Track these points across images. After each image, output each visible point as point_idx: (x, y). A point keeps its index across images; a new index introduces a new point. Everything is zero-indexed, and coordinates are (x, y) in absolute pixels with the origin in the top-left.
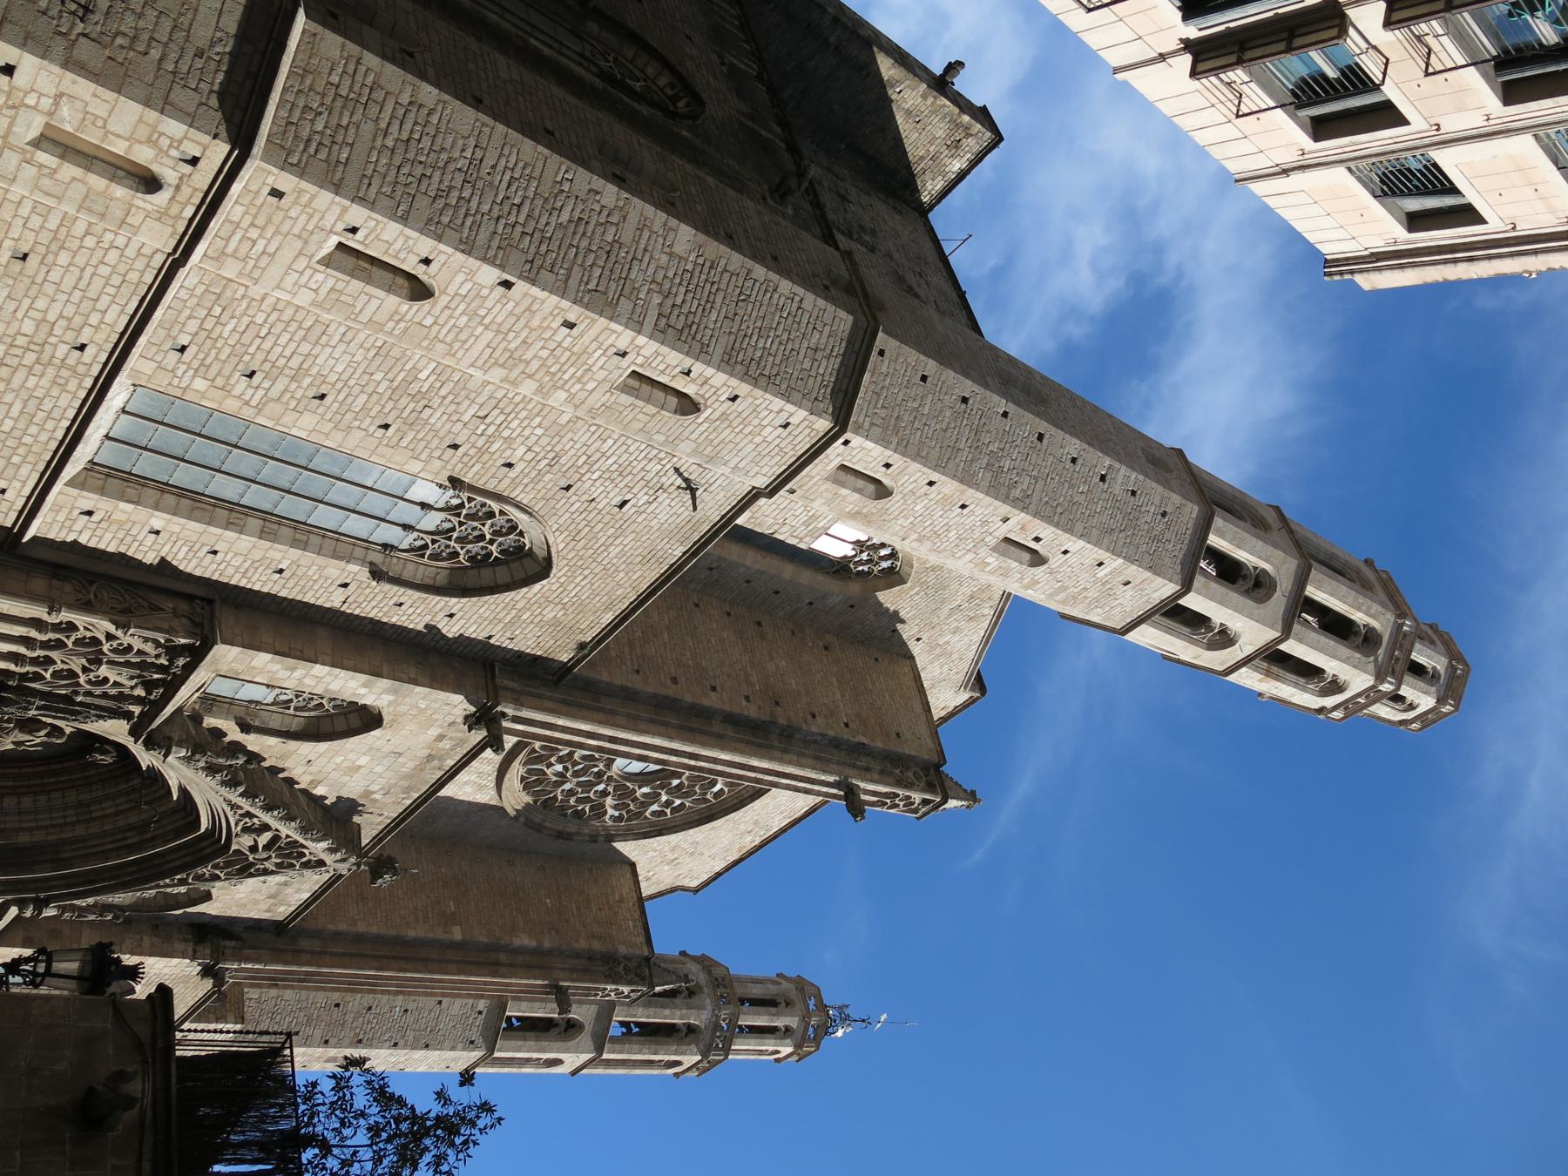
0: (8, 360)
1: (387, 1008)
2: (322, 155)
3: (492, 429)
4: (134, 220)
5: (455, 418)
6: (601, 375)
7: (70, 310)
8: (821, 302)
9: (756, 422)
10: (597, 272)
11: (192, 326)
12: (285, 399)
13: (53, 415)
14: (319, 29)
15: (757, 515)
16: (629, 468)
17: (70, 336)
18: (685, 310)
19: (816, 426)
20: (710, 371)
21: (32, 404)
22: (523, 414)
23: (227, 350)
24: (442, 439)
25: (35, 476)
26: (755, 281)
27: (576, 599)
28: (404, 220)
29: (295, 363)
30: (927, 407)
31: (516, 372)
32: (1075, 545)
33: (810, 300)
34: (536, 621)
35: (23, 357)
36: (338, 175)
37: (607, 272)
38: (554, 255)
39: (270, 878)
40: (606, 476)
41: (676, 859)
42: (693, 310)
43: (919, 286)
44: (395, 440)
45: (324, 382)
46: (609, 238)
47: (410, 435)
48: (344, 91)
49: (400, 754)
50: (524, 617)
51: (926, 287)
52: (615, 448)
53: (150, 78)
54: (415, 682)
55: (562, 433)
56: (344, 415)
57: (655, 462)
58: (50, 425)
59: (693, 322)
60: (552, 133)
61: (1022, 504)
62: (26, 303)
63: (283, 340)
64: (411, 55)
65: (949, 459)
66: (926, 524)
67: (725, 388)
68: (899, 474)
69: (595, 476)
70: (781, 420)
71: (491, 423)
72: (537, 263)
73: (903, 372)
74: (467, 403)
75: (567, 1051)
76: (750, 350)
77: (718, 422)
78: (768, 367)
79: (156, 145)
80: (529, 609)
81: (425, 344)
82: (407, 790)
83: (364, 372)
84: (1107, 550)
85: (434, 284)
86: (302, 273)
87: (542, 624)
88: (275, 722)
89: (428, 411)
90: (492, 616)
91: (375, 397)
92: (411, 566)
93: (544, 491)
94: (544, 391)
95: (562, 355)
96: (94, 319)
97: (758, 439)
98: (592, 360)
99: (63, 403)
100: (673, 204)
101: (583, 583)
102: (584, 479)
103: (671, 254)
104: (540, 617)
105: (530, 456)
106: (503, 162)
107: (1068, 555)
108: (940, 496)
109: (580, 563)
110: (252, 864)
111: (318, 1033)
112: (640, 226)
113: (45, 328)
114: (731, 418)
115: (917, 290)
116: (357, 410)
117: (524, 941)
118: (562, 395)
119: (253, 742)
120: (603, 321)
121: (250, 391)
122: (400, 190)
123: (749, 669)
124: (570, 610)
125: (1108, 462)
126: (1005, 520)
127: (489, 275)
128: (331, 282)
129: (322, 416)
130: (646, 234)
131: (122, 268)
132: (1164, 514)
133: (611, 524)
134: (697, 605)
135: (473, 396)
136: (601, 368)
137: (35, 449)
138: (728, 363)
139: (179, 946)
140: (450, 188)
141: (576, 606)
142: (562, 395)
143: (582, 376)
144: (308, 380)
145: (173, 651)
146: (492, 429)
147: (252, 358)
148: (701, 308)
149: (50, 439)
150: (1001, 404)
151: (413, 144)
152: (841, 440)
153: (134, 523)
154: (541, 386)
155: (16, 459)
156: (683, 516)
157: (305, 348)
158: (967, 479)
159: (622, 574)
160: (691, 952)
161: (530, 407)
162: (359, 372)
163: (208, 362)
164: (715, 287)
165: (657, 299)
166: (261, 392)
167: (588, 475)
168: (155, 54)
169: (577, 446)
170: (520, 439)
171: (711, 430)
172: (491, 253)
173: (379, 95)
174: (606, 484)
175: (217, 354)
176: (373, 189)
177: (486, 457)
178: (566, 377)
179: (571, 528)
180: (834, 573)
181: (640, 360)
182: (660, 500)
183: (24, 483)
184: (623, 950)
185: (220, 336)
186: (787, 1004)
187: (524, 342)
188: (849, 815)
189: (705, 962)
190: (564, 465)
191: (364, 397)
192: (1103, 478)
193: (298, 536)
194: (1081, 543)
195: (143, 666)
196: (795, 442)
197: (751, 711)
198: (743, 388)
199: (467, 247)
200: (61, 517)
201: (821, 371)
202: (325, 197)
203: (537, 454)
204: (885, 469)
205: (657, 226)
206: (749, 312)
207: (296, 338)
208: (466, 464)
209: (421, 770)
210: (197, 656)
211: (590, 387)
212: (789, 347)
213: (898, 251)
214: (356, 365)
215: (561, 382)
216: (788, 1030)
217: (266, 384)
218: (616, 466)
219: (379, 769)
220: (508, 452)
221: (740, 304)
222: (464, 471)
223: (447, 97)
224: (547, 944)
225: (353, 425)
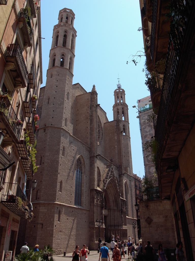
11: (69, 202)
20: (61, 147)
28: (56, 186)
29: (69, 191)
32: (66, 90)
54: (94, 166)
60: (41, 172)
61: (63, 99)
64: (39, 189)
75: (127, 126)
84: (65, 84)
100: (44, 156)
103: (50, 155)
111: (128, 158)
117: (116, 138)
120: (59, 161)
127: (59, 175)
130: (48, 159)
132: (59, 75)
134: (77, 130)
138: (59, 145)
139: (121, 179)
158: (63, 108)
165: (55, 156)
166: (73, 193)
184: (115, 124)
186: (118, 94)
189: (114, 107)
192: (57, 86)
194: (66, 88)
195: (98, 195)
197: (89, 122)
198: (61, 142)
199: (57, 179)
202: (57, 194)
224: (116, 135)
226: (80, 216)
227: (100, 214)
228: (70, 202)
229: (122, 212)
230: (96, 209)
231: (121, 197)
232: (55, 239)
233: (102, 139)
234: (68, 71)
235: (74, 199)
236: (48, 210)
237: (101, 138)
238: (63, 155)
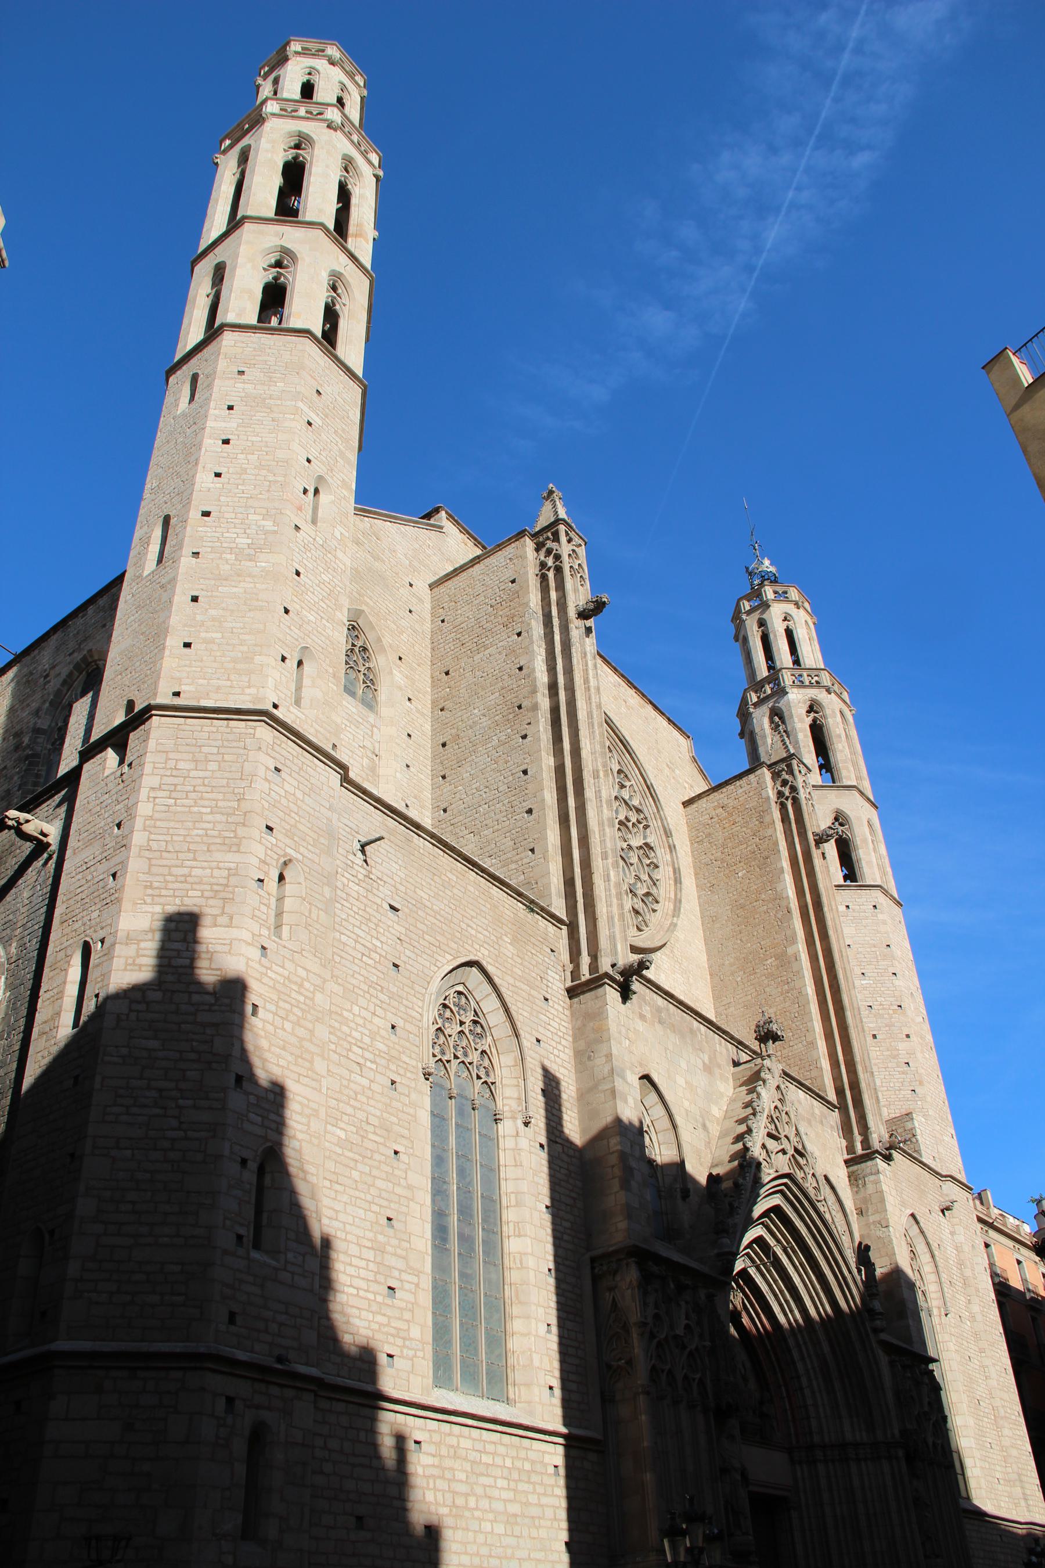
0: (449, 1502)
1: (865, 992)
3: (367, 1055)
5: (370, 1093)
6: (288, 964)
8: (148, 768)
9: (284, 801)
12: (404, 1253)
13: (481, 1449)
15: (364, 775)
16: (361, 912)
19: (270, 740)
22: (345, 1029)
23: (379, 1318)
24: (391, 1099)
26: (149, 840)
27: (489, 929)
29: (370, 1255)
30: (215, 635)
31: (313, 1048)
34: (519, 960)
35: (442, 1490)
38: (194, 1044)
39: (802, 1130)
40: (374, 933)
41: (668, 765)
42: (199, 894)
43: (59, 674)
44: (405, 1142)
45: (376, 1223)
49: (666, 1049)
50: (520, 973)
51: (57, 668)
52: (348, 933)
55: (351, 987)
56: (399, 1196)
57: (347, 890)
58: (490, 1448)
59: (212, 890)
60: (76, 1078)
65: (258, 600)
66: (324, 606)
67: (264, 841)
68: (287, 646)
69: (379, 944)
70: (272, 776)
71: (362, 1057)
73: (188, 669)
74: (352, 1085)
76: (219, 827)
77: (296, 838)
78: (229, 804)
80: (512, 971)
81: (316, 1141)
83: (356, 1189)
85: (261, 1149)
86: (293, 1273)
87: (520, 955)
89: (373, 1120)
90: (528, 1003)
91: (375, 1172)
93: (406, 989)
94: (320, 1015)
95: (284, 1009)
97: (299, 794)
98: (279, 978)
99: (465, 1443)
100: (102, 941)
101: (474, 926)
102: (384, 954)
104: (515, 957)
105: (379, 1011)
107: (311, 458)
108: (295, 599)
109: (457, 934)
110: (796, 1150)
111: (903, 1046)
112: (137, 968)
114: (288, 827)
115: (63, 676)
116: (390, 1185)
118: (319, 997)
121: (407, 1286)
123: (494, 743)
124: (500, 930)
125: (207, 442)
129: (406, 1214)
133: (415, 915)
135: (345, 1083)
136: (283, 967)
137: (514, 1454)
139: (871, 1188)
141: (495, 927)
142: (319, 997)
143: (296, 983)
144: (380, 1238)
146: (367, 1055)
147: (378, 1294)
148: (195, 886)
149: (502, 1444)
152: (275, 711)
153: (548, 1349)
154: (318, 1020)
155: (527, 1466)
156: (388, 848)
159: (455, 891)
160: (739, 729)
161: (337, 1025)
162: (357, 1193)
163: (393, 1331)
164: (169, 878)
166: (405, 1276)
167: (378, 950)
169: (357, 969)
170: (368, 1025)
171: (305, 844)
174: (382, 931)
175: (385, 1325)
177: (394, 1053)
178: (302, 999)
179: (429, 952)
180: (373, 684)
181: (265, 932)
182: (379, 875)
183: (544, 1452)
185: (368, 1328)
187: (284, 1048)
188: (604, 610)
190: (378, 977)
191: (379, 1183)
192: (226, 442)
193: (513, 1203)
196: (291, 758)
201: (215, 750)
203: (376, 1005)
204: (287, 661)
206: (181, 838)
207: (348, 1260)
208: (406, 1069)
209: (673, 1026)
211: (303, 973)
212: (201, 788)
213: (28, 705)
214: (353, 1199)
215: (308, 1001)
217: (396, 1273)
218: (364, 927)
219: (684, 1065)
220: (383, 1033)
221: (177, 849)
222: (412, 1069)
225: (405, 1184)
226: (510, 1495)
234: (312, 352)
237: (665, 906)
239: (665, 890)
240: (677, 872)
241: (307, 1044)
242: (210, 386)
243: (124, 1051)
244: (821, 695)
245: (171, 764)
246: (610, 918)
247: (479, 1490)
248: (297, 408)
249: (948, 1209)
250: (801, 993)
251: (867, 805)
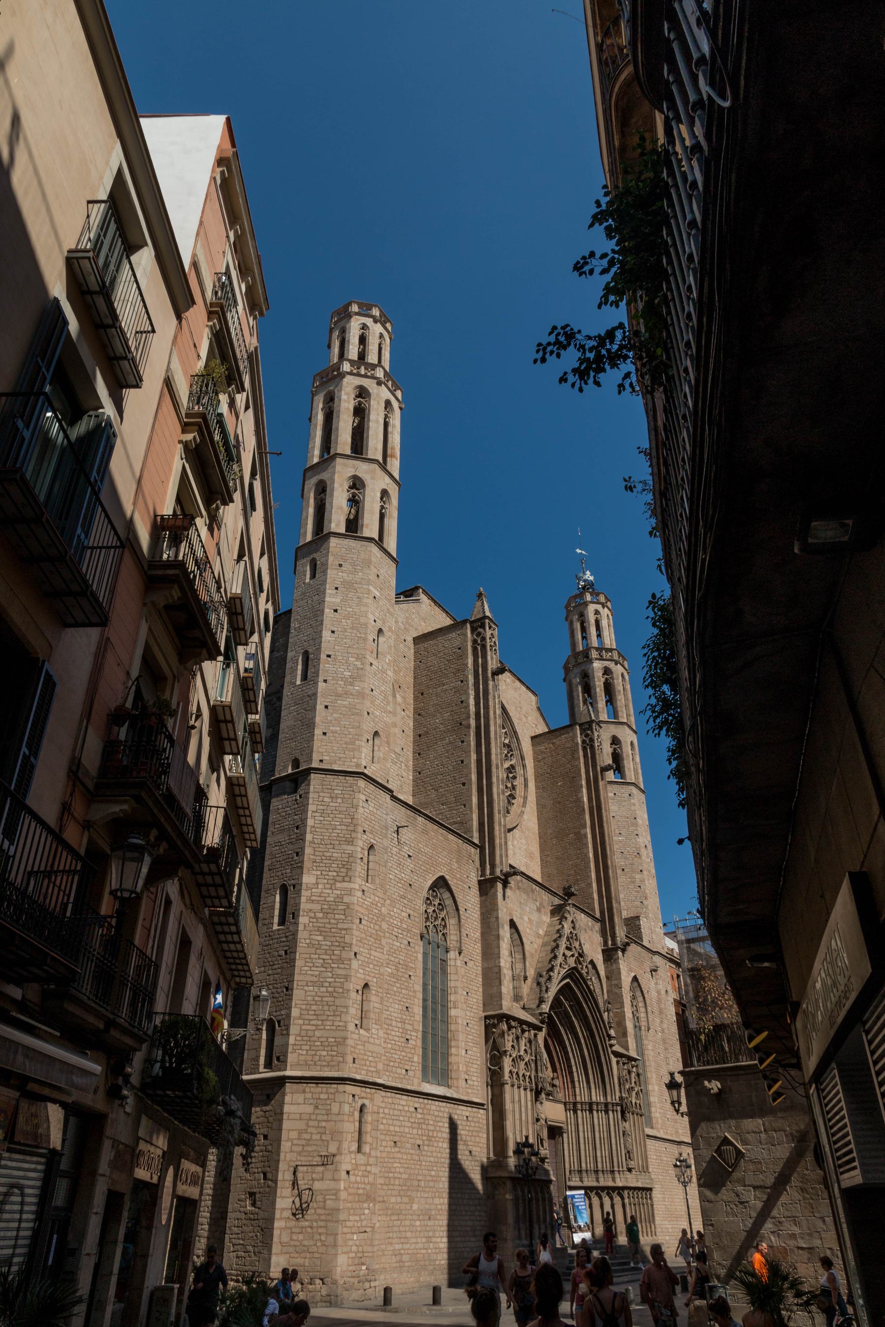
2: (335, 1049)
4: (376, 1110)
6: (372, 896)
7: (406, 1119)
10: (337, 916)
11: (399, 1071)
14: (288, 1064)
17: (414, 1115)
18: (337, 869)
21: (438, 1119)
23: (403, 1054)
25: (460, 1107)
28: (347, 1007)
29: (399, 1025)
33: (311, 808)
36: (340, 1040)
37: (335, 912)
39: (582, 942)
46: (321, 915)
47: (410, 964)
48: (308, 1047)
53: (333, 1123)
54: (497, 918)
58: (442, 1109)
60: (286, 951)
61: (361, 658)
62: (408, 1136)
63: (393, 1033)
70: (365, 805)
72: (342, 944)
76: (344, 832)
79: (353, 1113)
82: (533, 891)
88: (519, 966)
89: (401, 962)
92: (452, 937)
96: (406, 1108)
99: (433, 1108)
100: (294, 886)
103: (317, 883)
106: (309, 972)
110: (579, 954)
113: (414, 1125)
119: (531, 973)
120: (356, 907)
122: (337, 1013)
125: (327, 610)
126: (371, 664)
127: (355, 964)
128: (374, 1026)
130: (313, 898)
131: (389, 1106)
132: (340, 565)
140: (327, 992)
142: (383, 908)
144: (404, 1017)
145: (510, 1028)
150: (321, 685)
151: (317, 1013)
152: (366, 771)
157: (394, 1023)
160: (563, 676)
165: (338, 885)
166: (413, 1033)
168: (324, 1124)
172: (347, 967)
173: (304, 1033)
176: (341, 1024)
191: (404, 991)
192: (336, 611)
198: (360, 829)
199: (347, 977)
200: (470, 1091)
202: (350, 1042)
205: (308, 893)
210: (508, 1018)
211: (377, 899)
216: (597, 612)
219: (528, 910)
223: (293, 1004)
227: (530, 1121)
228: (404, 1071)
229: (623, 1113)
230: (513, 1102)
231: (618, 1043)
232: (345, 1230)
233: (524, 804)
235: (417, 1059)
236: (316, 1107)
237: (519, 801)
238: (370, 881)
239: (519, 791)
240: (526, 780)
241: (379, 932)
242: (325, 572)
243: (308, 941)
244: (611, 665)
245: (321, 799)
246: (501, 845)
247: (438, 1129)
248: (369, 590)
249: (655, 971)
250: (586, 856)
251: (631, 732)
